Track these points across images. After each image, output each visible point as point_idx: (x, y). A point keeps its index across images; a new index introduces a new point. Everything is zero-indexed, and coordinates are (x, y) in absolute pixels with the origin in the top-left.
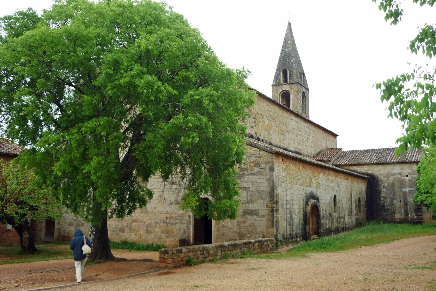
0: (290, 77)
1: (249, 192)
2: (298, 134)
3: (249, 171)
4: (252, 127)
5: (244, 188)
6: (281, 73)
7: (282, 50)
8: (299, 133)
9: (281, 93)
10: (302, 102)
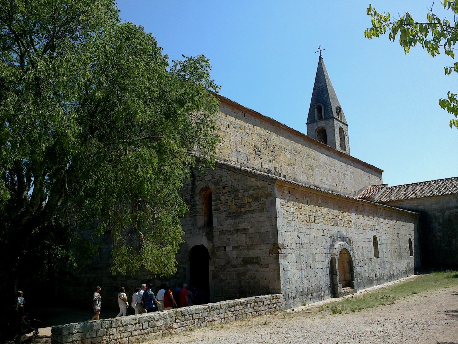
0: (324, 112)
1: (248, 234)
2: (331, 169)
3: (247, 208)
4: (270, 161)
5: (242, 229)
6: (316, 110)
7: (315, 86)
8: (332, 168)
9: (316, 131)
10: (341, 139)
